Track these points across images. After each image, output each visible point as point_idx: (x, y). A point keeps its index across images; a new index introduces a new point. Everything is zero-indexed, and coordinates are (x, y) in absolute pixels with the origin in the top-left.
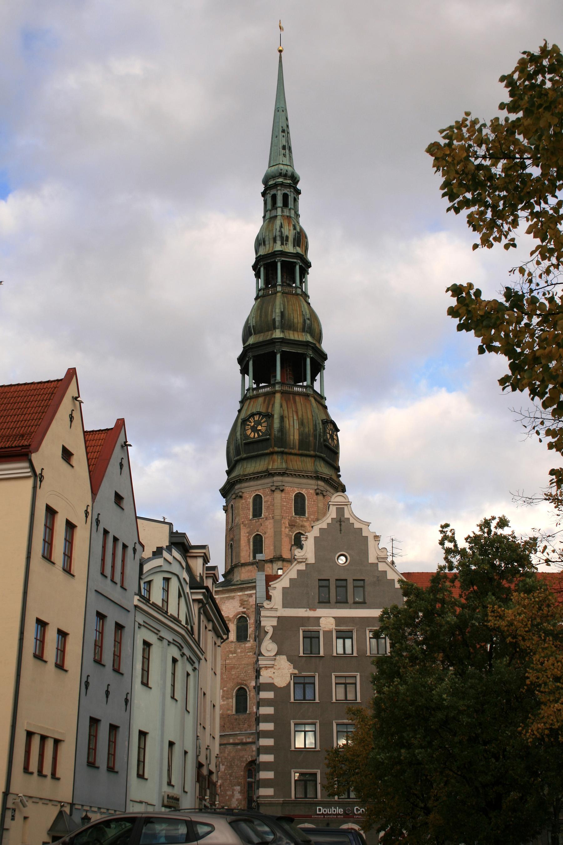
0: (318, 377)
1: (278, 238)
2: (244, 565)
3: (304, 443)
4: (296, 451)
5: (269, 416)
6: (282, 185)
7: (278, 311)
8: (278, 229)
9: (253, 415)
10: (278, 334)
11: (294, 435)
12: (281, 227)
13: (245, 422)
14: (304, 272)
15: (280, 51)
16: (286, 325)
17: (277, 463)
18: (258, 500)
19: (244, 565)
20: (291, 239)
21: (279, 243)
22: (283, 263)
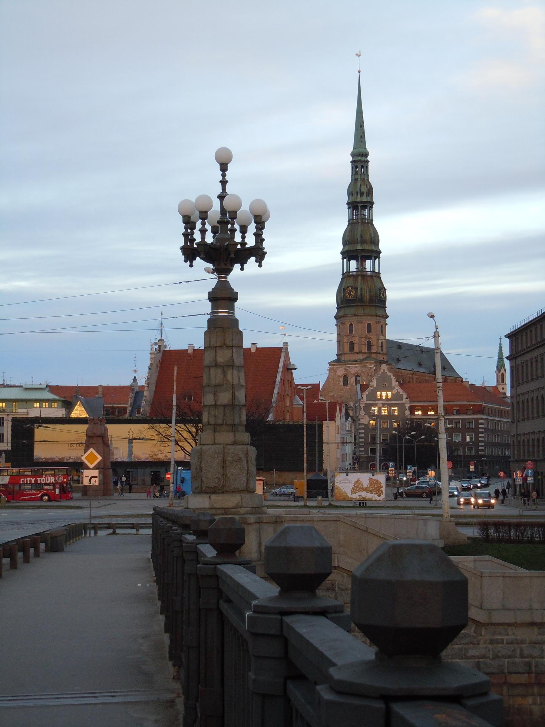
0: (377, 259)
1: (359, 193)
2: (346, 354)
3: (371, 301)
4: (367, 304)
5: (356, 289)
6: (361, 161)
7: (359, 235)
8: (359, 187)
9: (348, 287)
10: (359, 247)
11: (367, 297)
12: (360, 187)
13: (345, 290)
14: (371, 207)
15: (359, 72)
16: (363, 242)
17: (360, 311)
18: (351, 325)
19: (346, 354)
20: (365, 194)
21: (359, 195)
22: (361, 206)
